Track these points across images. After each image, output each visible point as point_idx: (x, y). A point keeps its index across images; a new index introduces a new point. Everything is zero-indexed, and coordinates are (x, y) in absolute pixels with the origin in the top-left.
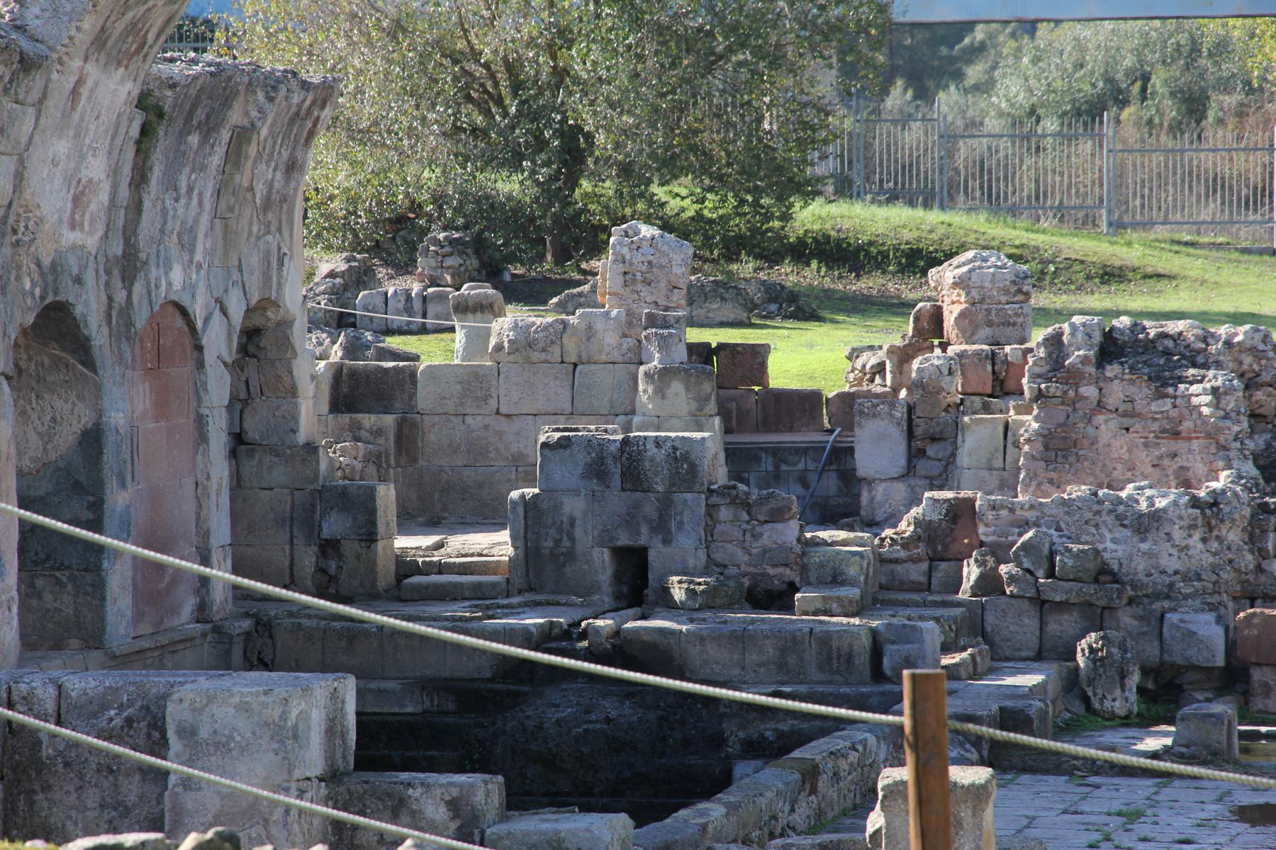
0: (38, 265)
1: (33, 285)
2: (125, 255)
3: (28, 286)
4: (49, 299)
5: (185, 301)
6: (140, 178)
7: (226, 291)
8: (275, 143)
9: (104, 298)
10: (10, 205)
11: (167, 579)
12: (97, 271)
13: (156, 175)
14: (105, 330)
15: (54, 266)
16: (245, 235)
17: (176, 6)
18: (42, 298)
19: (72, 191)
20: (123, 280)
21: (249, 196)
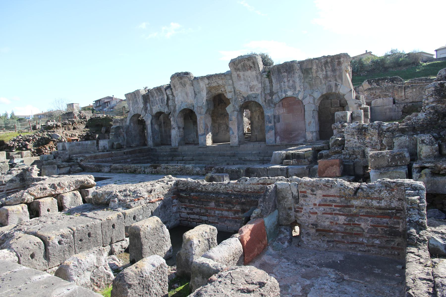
0: (243, 97)
1: (242, 99)
2: (270, 92)
3: (240, 100)
4: (247, 101)
5: (295, 96)
6: (271, 82)
7: (312, 93)
8: (322, 68)
9: (264, 99)
10: (234, 91)
11: (293, 136)
12: (262, 96)
13: (274, 81)
14: (264, 103)
15: (248, 97)
16: (319, 83)
17: (252, 61)
18: (244, 101)
19: (249, 87)
20: (270, 96)
21: (318, 77)
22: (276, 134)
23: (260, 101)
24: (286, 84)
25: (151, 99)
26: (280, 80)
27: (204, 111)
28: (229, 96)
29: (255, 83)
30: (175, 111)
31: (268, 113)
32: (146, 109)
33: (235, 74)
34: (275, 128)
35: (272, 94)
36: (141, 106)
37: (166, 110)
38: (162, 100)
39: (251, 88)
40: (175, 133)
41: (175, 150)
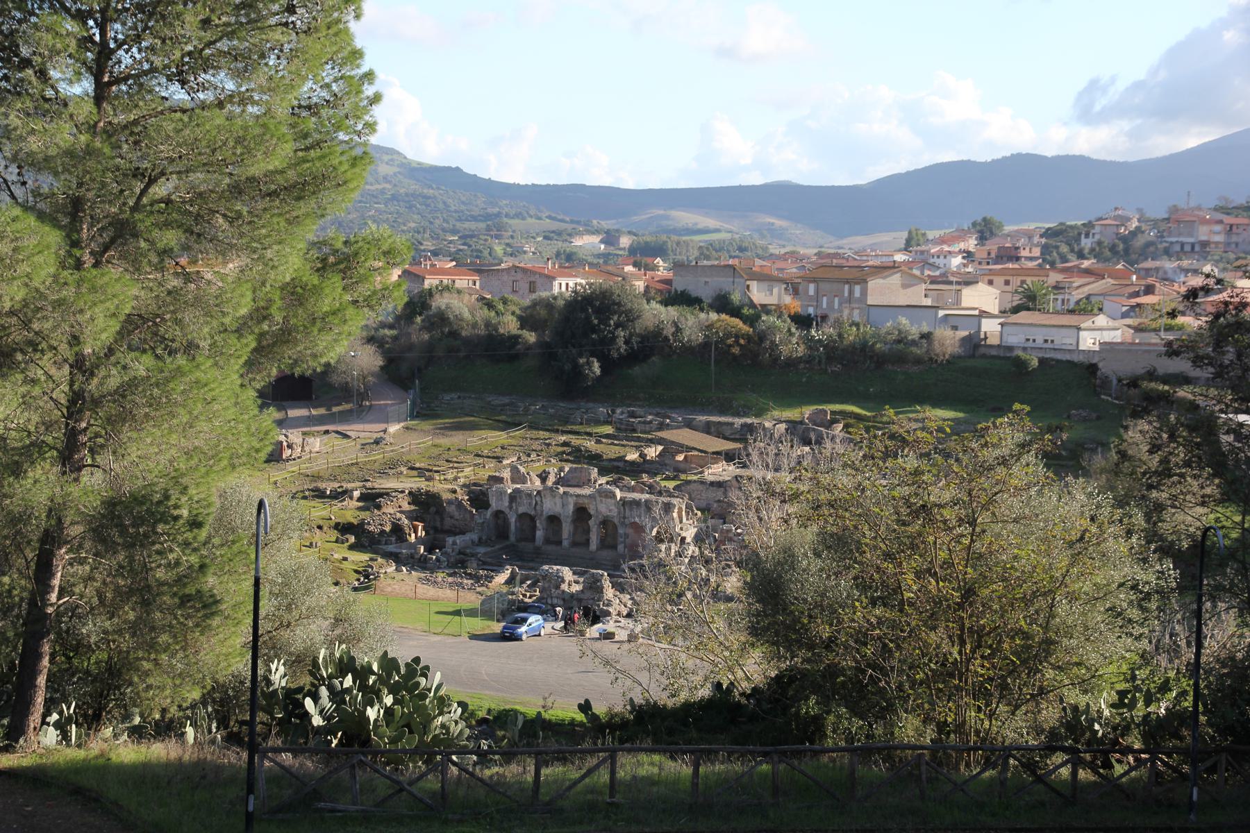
22: (625, 547)
23: (616, 521)
24: (635, 512)
25: (518, 500)
26: (631, 510)
27: (569, 520)
28: (592, 512)
29: (613, 507)
30: (541, 515)
31: (621, 531)
32: (511, 508)
33: (598, 499)
34: (624, 542)
35: (624, 518)
36: (507, 504)
37: (533, 513)
38: (530, 504)
39: (610, 511)
40: (539, 534)
41: (538, 548)
